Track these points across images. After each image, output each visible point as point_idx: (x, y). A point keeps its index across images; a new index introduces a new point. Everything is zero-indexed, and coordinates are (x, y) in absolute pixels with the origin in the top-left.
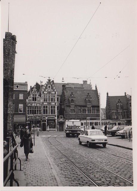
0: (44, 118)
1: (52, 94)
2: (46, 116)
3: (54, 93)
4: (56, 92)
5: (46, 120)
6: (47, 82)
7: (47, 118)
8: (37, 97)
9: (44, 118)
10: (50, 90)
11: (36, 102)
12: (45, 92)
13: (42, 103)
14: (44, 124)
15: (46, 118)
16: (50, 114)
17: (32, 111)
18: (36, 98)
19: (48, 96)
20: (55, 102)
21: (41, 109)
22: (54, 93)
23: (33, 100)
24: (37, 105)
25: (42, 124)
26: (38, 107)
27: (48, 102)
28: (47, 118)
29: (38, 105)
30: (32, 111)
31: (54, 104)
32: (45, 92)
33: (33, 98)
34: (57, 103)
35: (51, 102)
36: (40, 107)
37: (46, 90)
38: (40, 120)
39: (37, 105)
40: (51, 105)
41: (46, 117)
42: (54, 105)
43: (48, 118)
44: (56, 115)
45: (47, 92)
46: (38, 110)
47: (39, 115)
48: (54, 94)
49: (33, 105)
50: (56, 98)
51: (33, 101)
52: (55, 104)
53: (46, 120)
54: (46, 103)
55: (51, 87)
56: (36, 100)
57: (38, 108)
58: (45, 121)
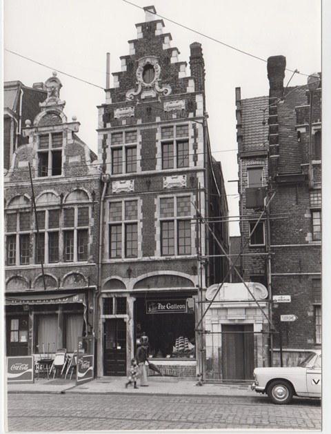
0: (115, 283)
1: (166, 115)
2: (130, 274)
3: (182, 104)
4: (193, 95)
5: (131, 302)
6: (134, 42)
7: (134, 281)
8: (63, 148)
9: (115, 283)
10: (152, 94)
11: (62, 178)
12: (118, 113)
13: (95, 186)
14: (116, 329)
15: (130, 285)
16: (157, 257)
17: (61, 236)
18: (57, 155)
19: (142, 132)
20: (192, 166)
21: (87, 223)
22: (182, 104)
23: (43, 173)
24: (62, 196)
25: (101, 322)
26: (69, 211)
27: (139, 171)
28: (134, 281)
29: (72, 198)
30: (61, 236)
31: (181, 180)
32: (118, 113)
33: (43, 156)
34: (200, 176)
35: (158, 169)
36: (83, 209)
37: (129, 95)
38: (76, 299)
39: (62, 196)
40: (164, 191)
41: (126, 281)
42: (184, 189)
43: (137, 285)
45: (130, 111)
46: (68, 234)
47: (75, 262)
48: (183, 115)
49: (42, 201)
51: (40, 175)
52: (193, 180)
53: (131, 302)
54: (128, 185)
55: (158, 68)
56: (57, 171)
57: (69, 222)
58: (122, 308)
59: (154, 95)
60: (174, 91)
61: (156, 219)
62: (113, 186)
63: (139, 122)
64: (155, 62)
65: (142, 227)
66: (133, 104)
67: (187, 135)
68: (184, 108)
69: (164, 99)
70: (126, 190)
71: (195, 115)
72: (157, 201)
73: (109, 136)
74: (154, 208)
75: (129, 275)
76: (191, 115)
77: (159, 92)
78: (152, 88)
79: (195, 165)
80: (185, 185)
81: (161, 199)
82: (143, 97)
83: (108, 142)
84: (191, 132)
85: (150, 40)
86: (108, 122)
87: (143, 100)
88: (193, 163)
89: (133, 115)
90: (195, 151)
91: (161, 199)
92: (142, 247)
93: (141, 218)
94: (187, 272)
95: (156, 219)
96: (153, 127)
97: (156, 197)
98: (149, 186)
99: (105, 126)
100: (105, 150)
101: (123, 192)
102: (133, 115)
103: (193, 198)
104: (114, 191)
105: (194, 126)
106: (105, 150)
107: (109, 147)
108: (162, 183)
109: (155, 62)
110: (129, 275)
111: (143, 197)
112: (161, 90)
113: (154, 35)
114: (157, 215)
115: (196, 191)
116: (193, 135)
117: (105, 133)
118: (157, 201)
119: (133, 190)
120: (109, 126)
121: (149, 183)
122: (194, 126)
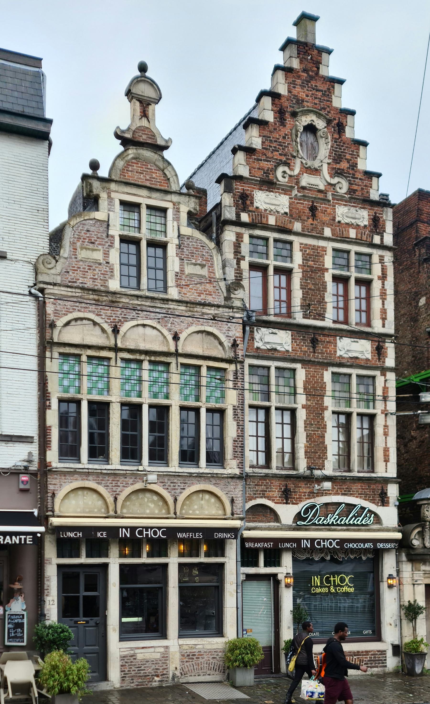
19: (304, 248)
44: (386, 481)
50: (383, 277)
59: (322, 187)
60: (351, 191)
61: (326, 408)
62: (257, 336)
63: (297, 226)
64: (320, 124)
65: (304, 418)
66: (286, 190)
67: (370, 271)
68: (366, 223)
69: (338, 198)
70: (279, 348)
71: (382, 239)
72: (327, 376)
73: (246, 239)
74: (323, 387)
75: (287, 499)
76: (377, 240)
77: (330, 184)
78: (316, 171)
79: (384, 326)
80: (370, 357)
81: (333, 373)
82: (303, 183)
83: (245, 248)
84: (377, 270)
85: (312, 78)
86: (244, 210)
87: (304, 188)
88: (381, 321)
89: (287, 210)
90: (383, 304)
91: (333, 373)
92: (306, 452)
93: (304, 403)
94: (373, 501)
95: (326, 408)
96: (322, 243)
97: (327, 370)
98: (314, 347)
99: (238, 216)
100: (238, 263)
101: (275, 350)
102: (287, 210)
103: (380, 381)
104: (256, 345)
105: (381, 259)
106: (238, 263)
107: (247, 259)
108: (336, 346)
109: (320, 124)
110: (287, 499)
111: (305, 363)
112: (334, 181)
113: (317, 73)
114: (328, 402)
115: (384, 370)
116: (380, 274)
117: (238, 229)
118: (327, 376)
119: (290, 350)
120: (245, 217)
121: (314, 342)
122: (381, 259)
